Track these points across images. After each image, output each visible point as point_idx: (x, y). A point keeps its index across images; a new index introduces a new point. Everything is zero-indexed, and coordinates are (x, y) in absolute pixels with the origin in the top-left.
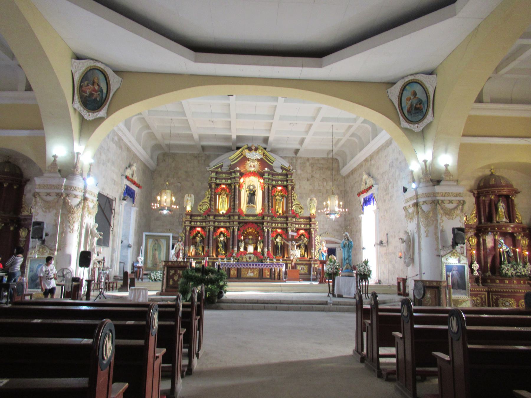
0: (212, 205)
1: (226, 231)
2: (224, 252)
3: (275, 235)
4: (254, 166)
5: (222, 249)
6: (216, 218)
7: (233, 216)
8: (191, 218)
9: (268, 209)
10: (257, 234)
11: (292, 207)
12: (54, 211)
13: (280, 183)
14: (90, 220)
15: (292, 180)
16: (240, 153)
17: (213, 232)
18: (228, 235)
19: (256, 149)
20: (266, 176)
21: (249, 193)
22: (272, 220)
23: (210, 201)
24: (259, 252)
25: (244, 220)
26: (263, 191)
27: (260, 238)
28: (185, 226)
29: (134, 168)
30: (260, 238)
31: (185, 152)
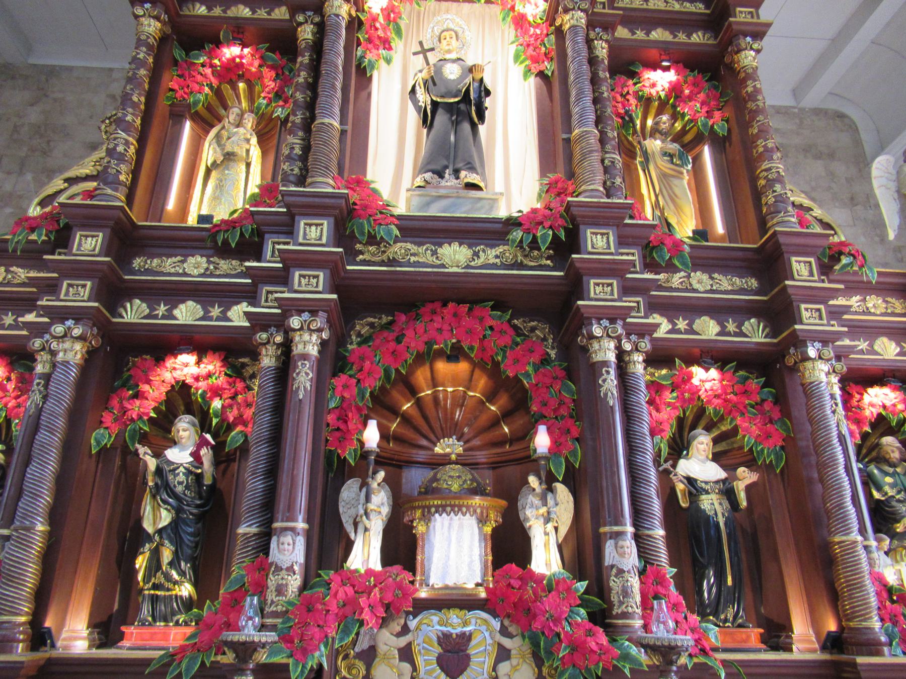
0: (121, 158)
1: (220, 380)
2: (186, 590)
3: (668, 416)
5: (167, 555)
6: (137, 262)
10: (506, 415)
17: (81, 385)
18: (240, 420)
21: (435, 104)
24: (551, 586)
25: (392, 262)
26: (541, 74)
27: (542, 441)
30: (542, 441)
31: (107, 65)
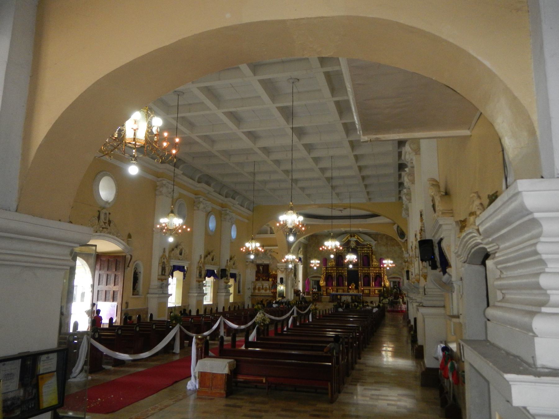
4: (353, 244)
7: (345, 267)
8: (326, 269)
9: (361, 264)
11: (372, 263)
12: (284, 274)
13: (366, 251)
14: (293, 275)
15: (372, 251)
16: (347, 238)
19: (354, 236)
20: (359, 248)
22: (363, 269)
23: (334, 260)
28: (324, 273)
29: (301, 249)
